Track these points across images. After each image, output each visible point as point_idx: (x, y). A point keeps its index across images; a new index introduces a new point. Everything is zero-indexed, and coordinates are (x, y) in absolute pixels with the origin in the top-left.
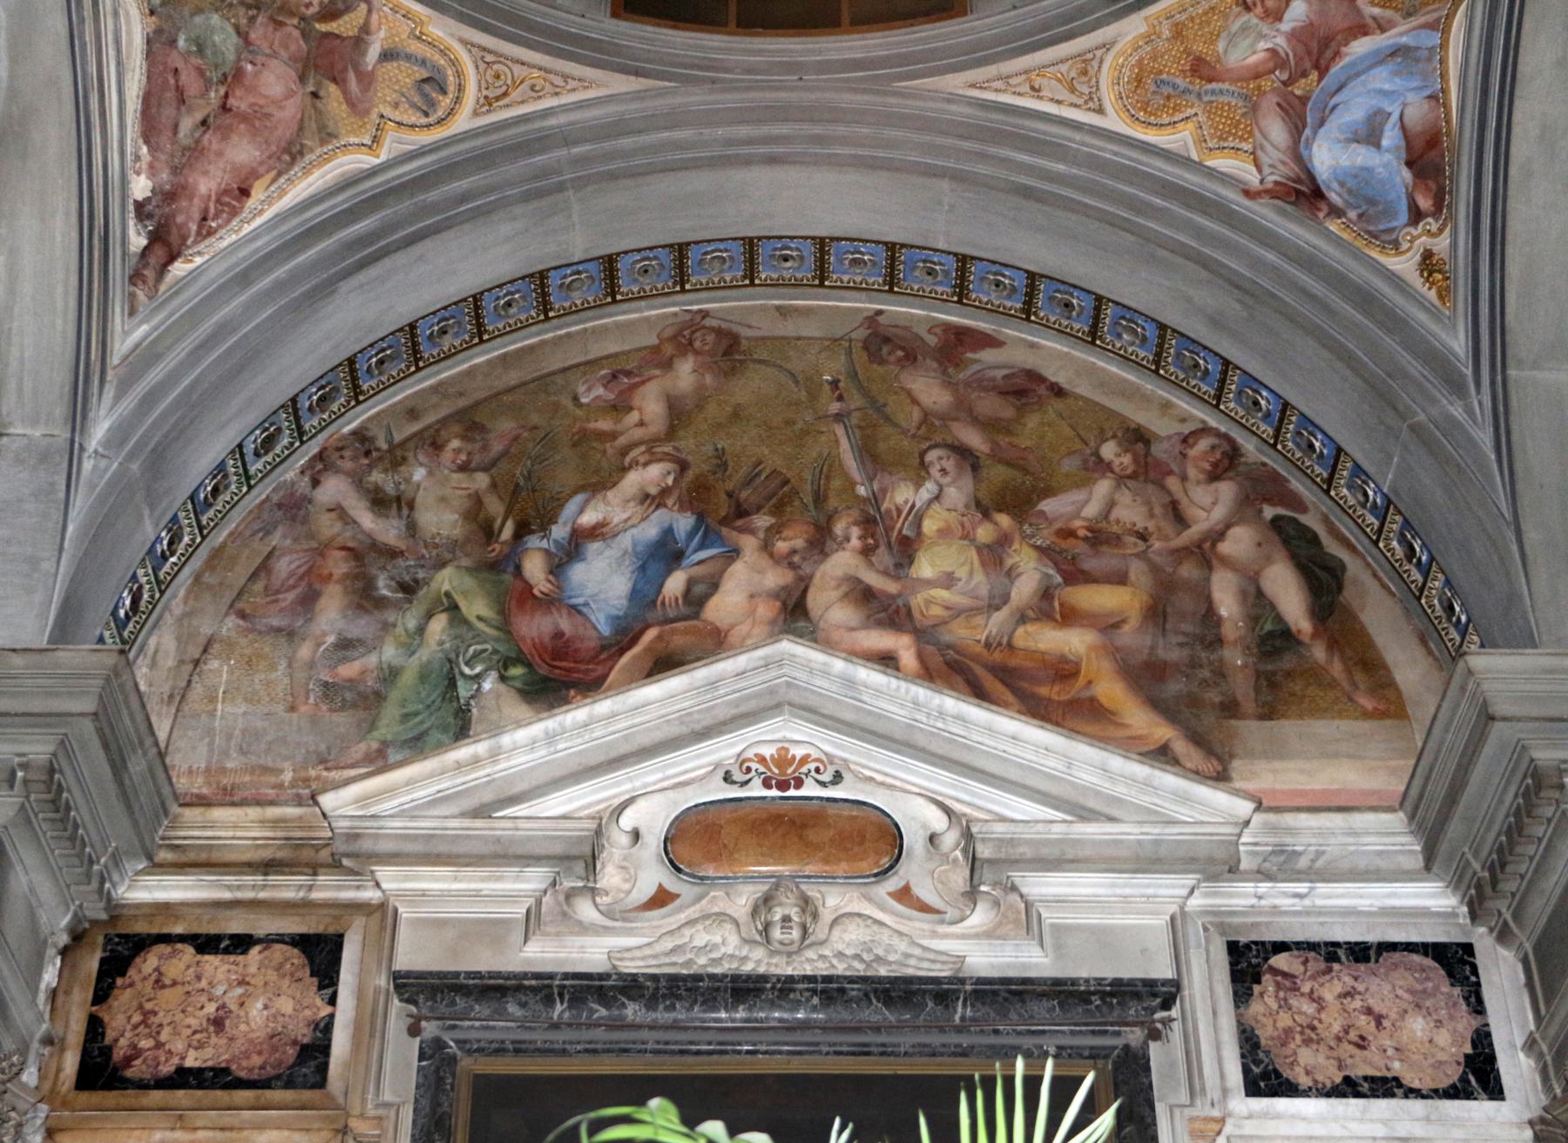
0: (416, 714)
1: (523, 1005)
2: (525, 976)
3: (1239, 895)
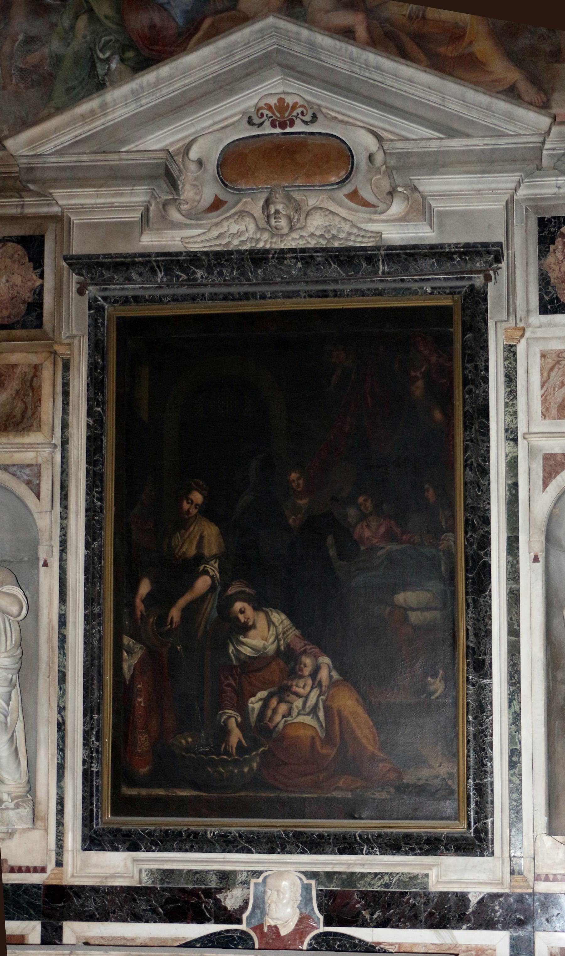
0: (74, 88)
1: (140, 274)
3: (549, 186)
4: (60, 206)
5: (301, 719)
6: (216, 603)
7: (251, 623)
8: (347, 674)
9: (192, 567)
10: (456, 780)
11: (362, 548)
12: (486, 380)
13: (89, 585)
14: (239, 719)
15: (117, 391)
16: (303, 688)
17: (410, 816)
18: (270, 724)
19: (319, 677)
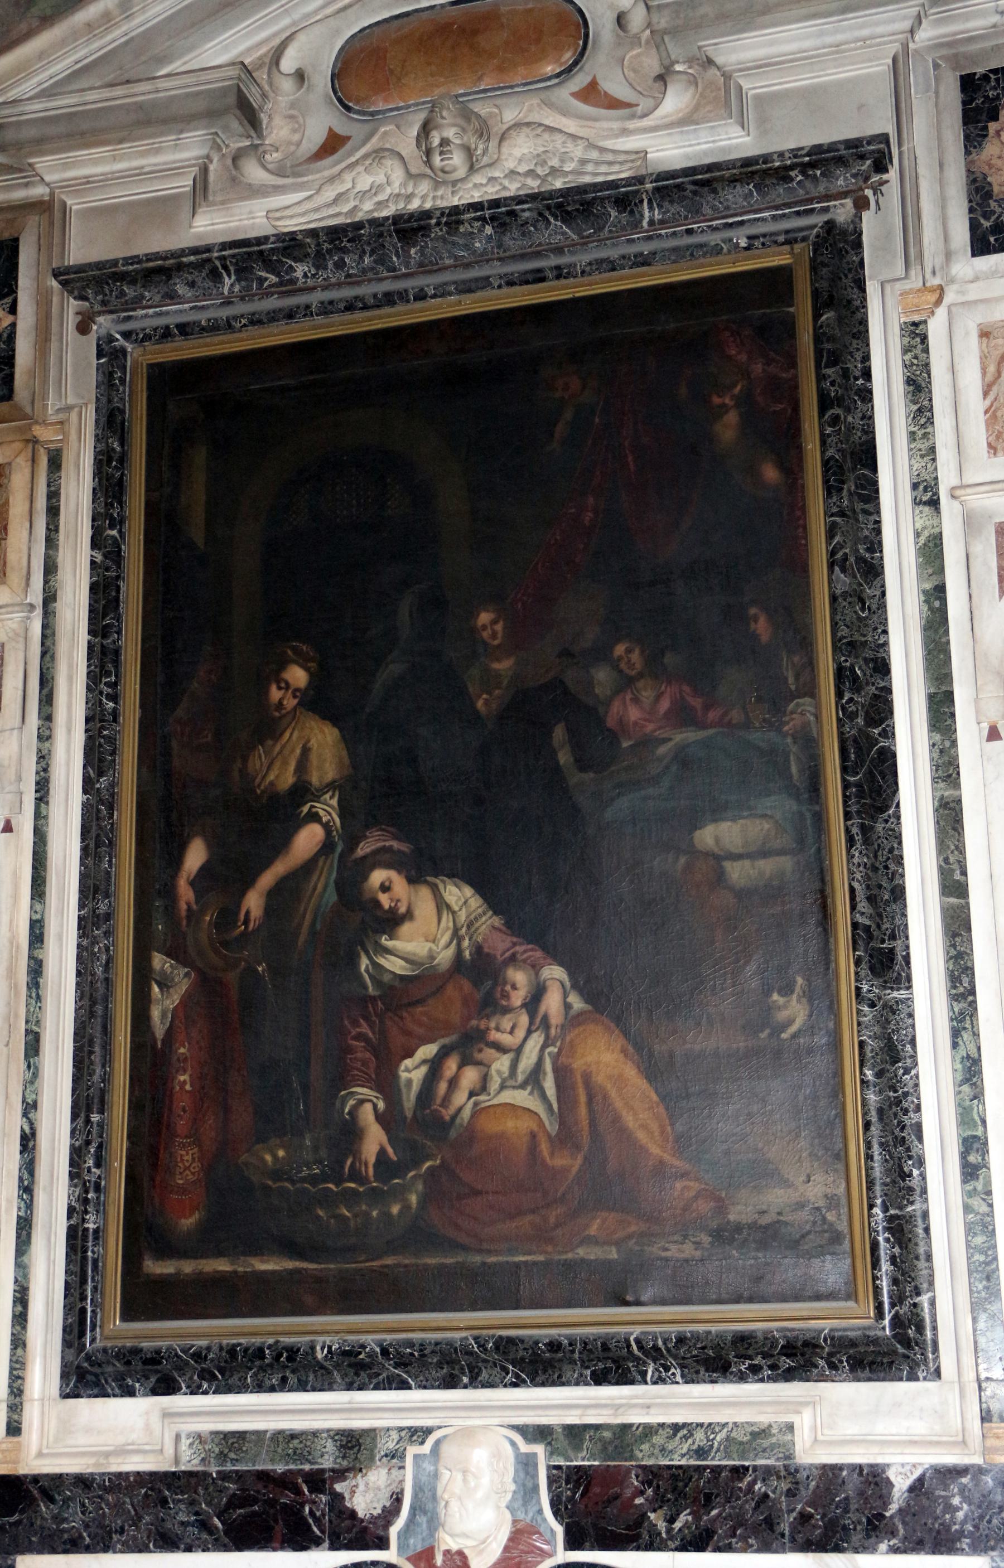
1: (192, 285)
2: (183, 252)
4: (48, 185)
5: (508, 1097)
6: (334, 875)
7: (403, 909)
8: (602, 997)
9: (288, 809)
10: (844, 1211)
11: (625, 744)
12: (867, 395)
13: (89, 861)
14: (381, 1105)
15: (146, 495)
16: (511, 1032)
17: (746, 1294)
18: (443, 1111)
19: (542, 1009)
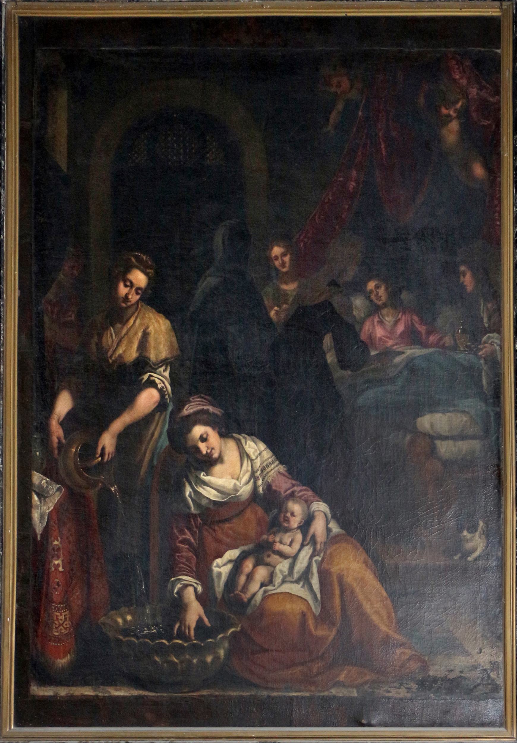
5: (287, 588)
6: (167, 426)
7: (216, 455)
9: (132, 376)
10: (501, 672)
14: (200, 589)
15: (21, 124)
16: (290, 545)
17: (438, 721)
18: (243, 595)
19: (312, 531)
